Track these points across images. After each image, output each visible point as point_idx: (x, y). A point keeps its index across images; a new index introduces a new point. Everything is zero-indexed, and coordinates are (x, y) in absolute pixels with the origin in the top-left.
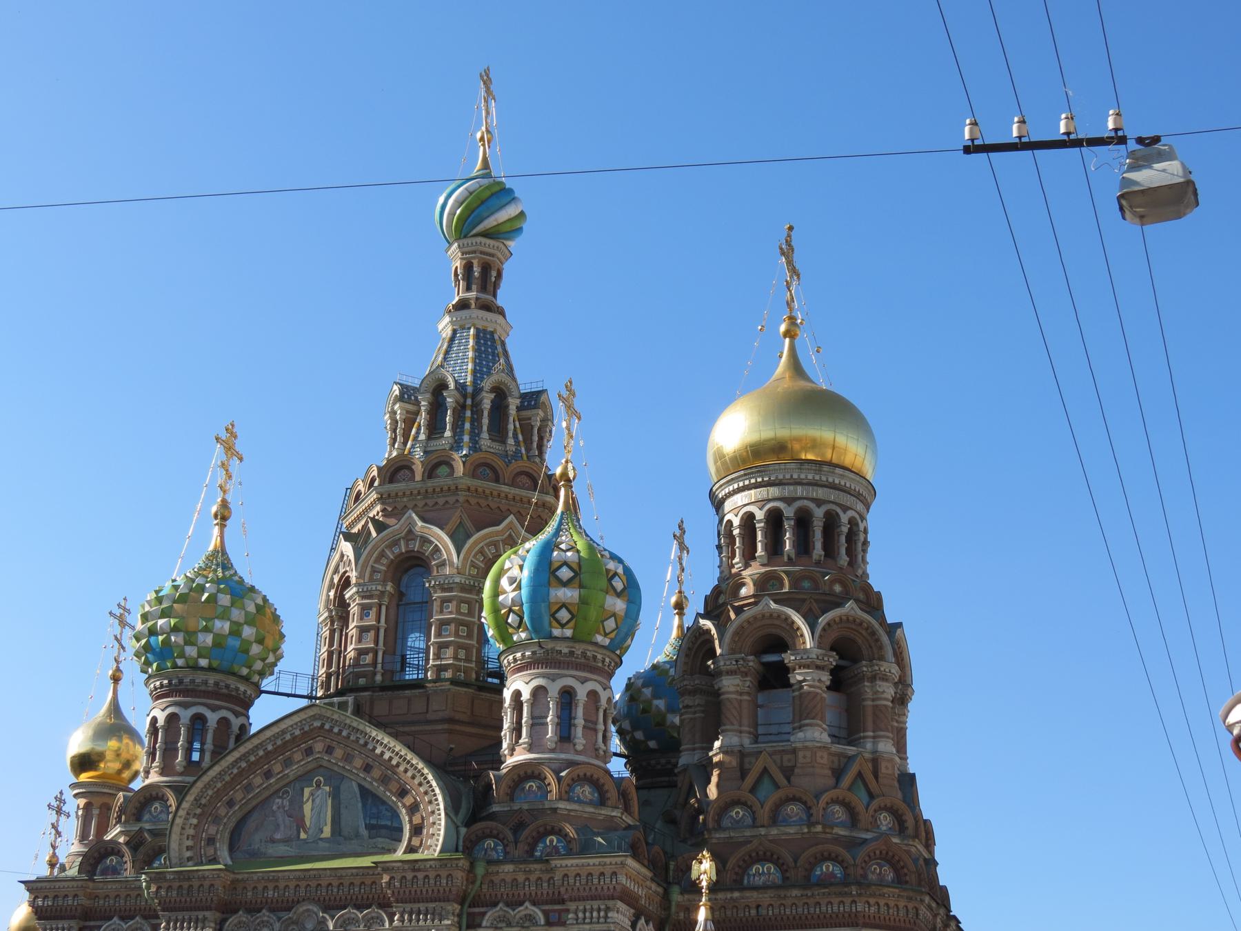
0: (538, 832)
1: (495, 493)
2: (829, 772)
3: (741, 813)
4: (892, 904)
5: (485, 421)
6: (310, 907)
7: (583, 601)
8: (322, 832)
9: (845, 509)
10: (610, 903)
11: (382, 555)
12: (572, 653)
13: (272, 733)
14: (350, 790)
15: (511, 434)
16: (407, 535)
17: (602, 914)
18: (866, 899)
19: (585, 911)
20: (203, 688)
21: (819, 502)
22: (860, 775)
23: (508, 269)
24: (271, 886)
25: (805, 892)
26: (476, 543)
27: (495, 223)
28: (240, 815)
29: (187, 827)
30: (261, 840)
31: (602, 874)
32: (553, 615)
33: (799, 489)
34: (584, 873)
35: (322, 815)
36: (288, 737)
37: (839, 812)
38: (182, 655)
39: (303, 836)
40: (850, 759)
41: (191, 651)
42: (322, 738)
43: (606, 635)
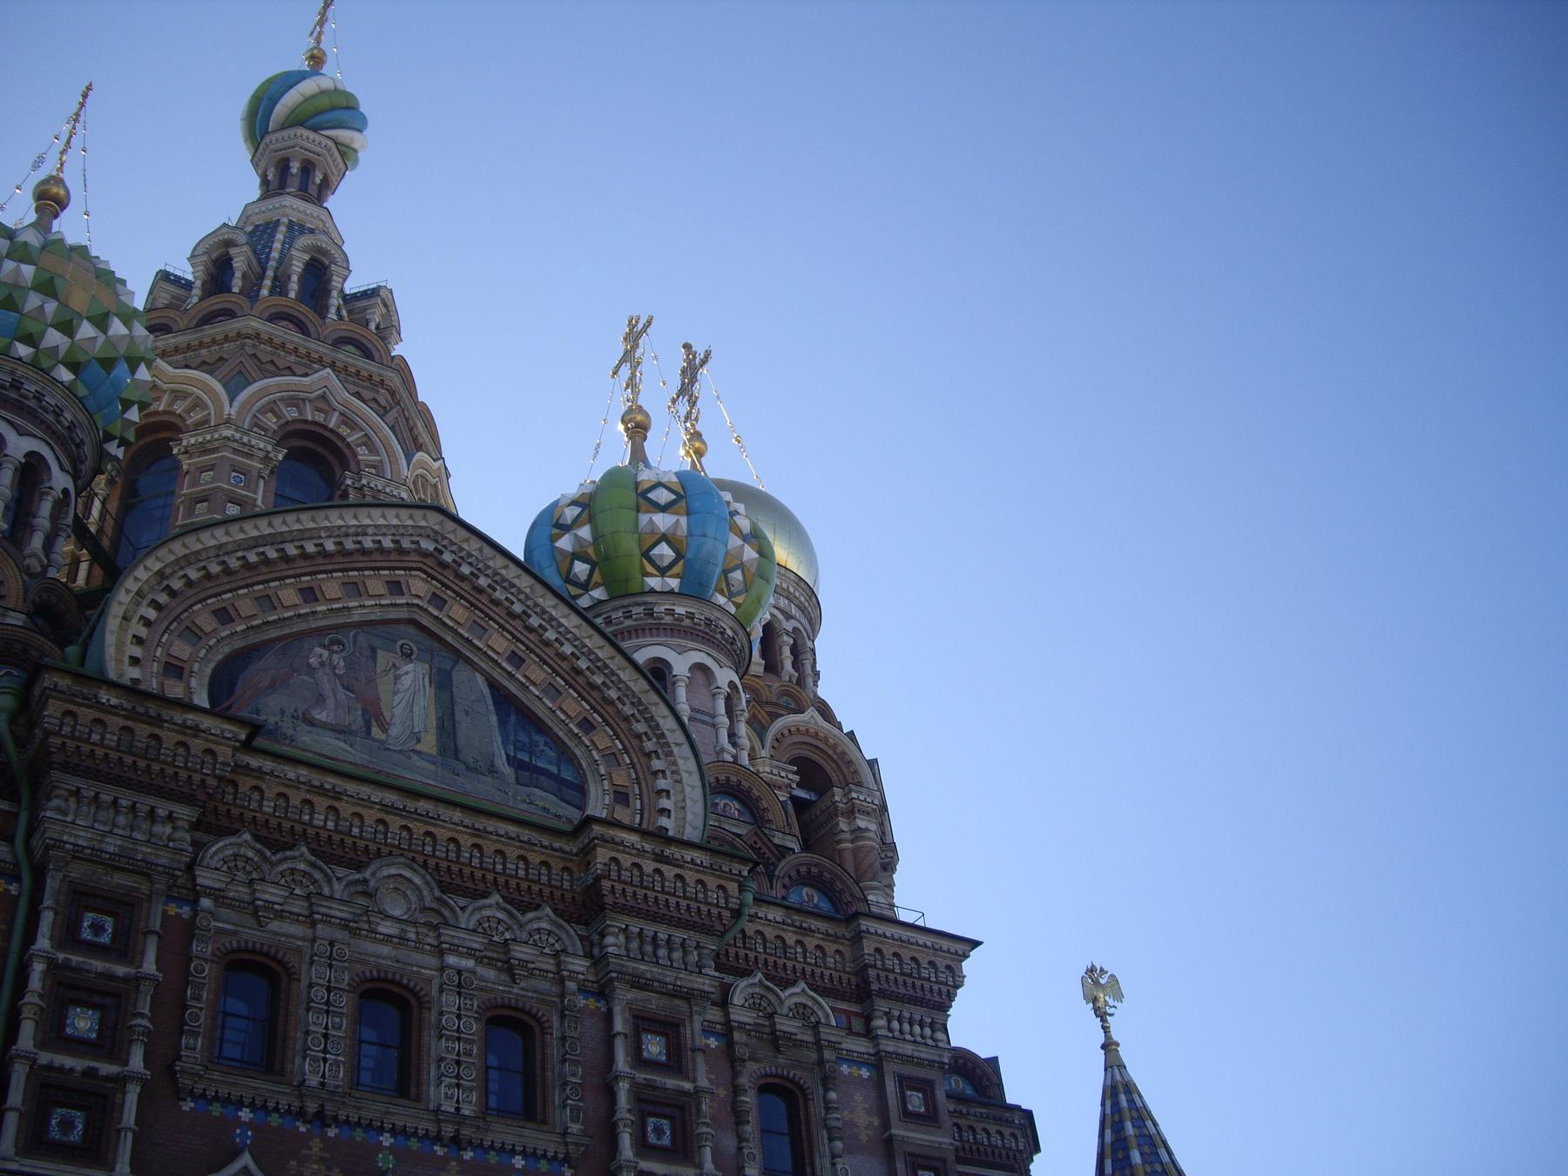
6: (407, 873)
8: (419, 741)
11: (271, 408)
13: (340, 523)
14: (471, 688)
20: (50, 418)
24: (321, 803)
27: (347, 142)
28: (238, 644)
29: (135, 620)
30: (283, 712)
31: (931, 963)
32: (725, 572)
33: (794, 610)
35: (416, 709)
36: (368, 543)
42: (424, 576)
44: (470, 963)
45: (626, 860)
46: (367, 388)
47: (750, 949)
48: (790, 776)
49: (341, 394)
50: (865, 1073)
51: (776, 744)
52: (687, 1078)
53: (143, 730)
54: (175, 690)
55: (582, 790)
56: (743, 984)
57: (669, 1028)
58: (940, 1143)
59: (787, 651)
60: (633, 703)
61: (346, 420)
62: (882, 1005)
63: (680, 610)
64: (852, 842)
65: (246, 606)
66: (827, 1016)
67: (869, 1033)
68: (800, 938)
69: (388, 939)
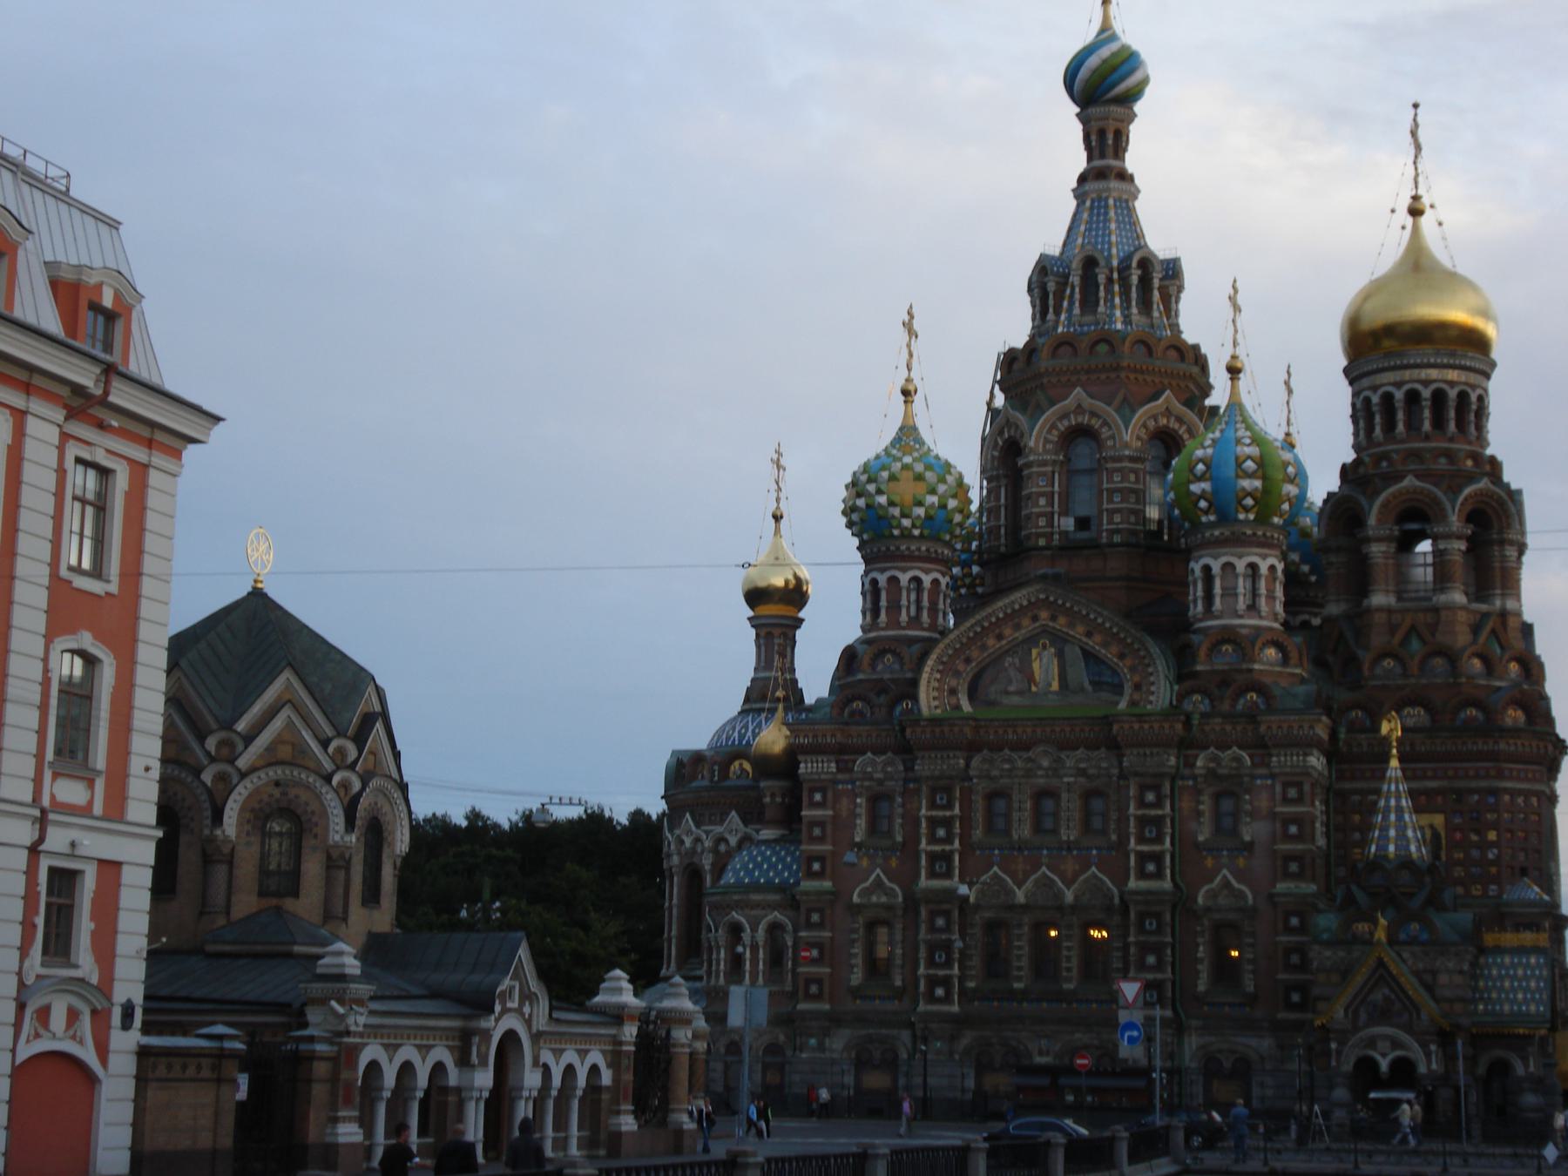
1: (1151, 368)
2: (1468, 629)
3: (1392, 664)
4: (1527, 743)
5: (1134, 295)
7: (1266, 490)
9: (1474, 387)
11: (1053, 426)
12: (1254, 534)
14: (1073, 653)
15: (1155, 306)
16: (1077, 408)
17: (1301, 758)
19: (1286, 755)
20: (917, 553)
21: (1452, 384)
22: (1493, 631)
23: (1135, 130)
26: (1140, 417)
29: (932, 681)
33: (1433, 373)
34: (1285, 726)
38: (899, 526)
39: (1034, 689)
40: (1485, 616)
41: (906, 522)
43: (1281, 516)
44: (1072, 779)
45: (1126, 726)
49: (1088, 402)
50: (1269, 782)
53: (937, 730)
54: (954, 701)
57: (1157, 788)
59: (1427, 413)
61: (1093, 414)
62: (1274, 751)
63: (1217, 533)
65: (975, 653)
67: (1268, 765)
69: (1042, 776)
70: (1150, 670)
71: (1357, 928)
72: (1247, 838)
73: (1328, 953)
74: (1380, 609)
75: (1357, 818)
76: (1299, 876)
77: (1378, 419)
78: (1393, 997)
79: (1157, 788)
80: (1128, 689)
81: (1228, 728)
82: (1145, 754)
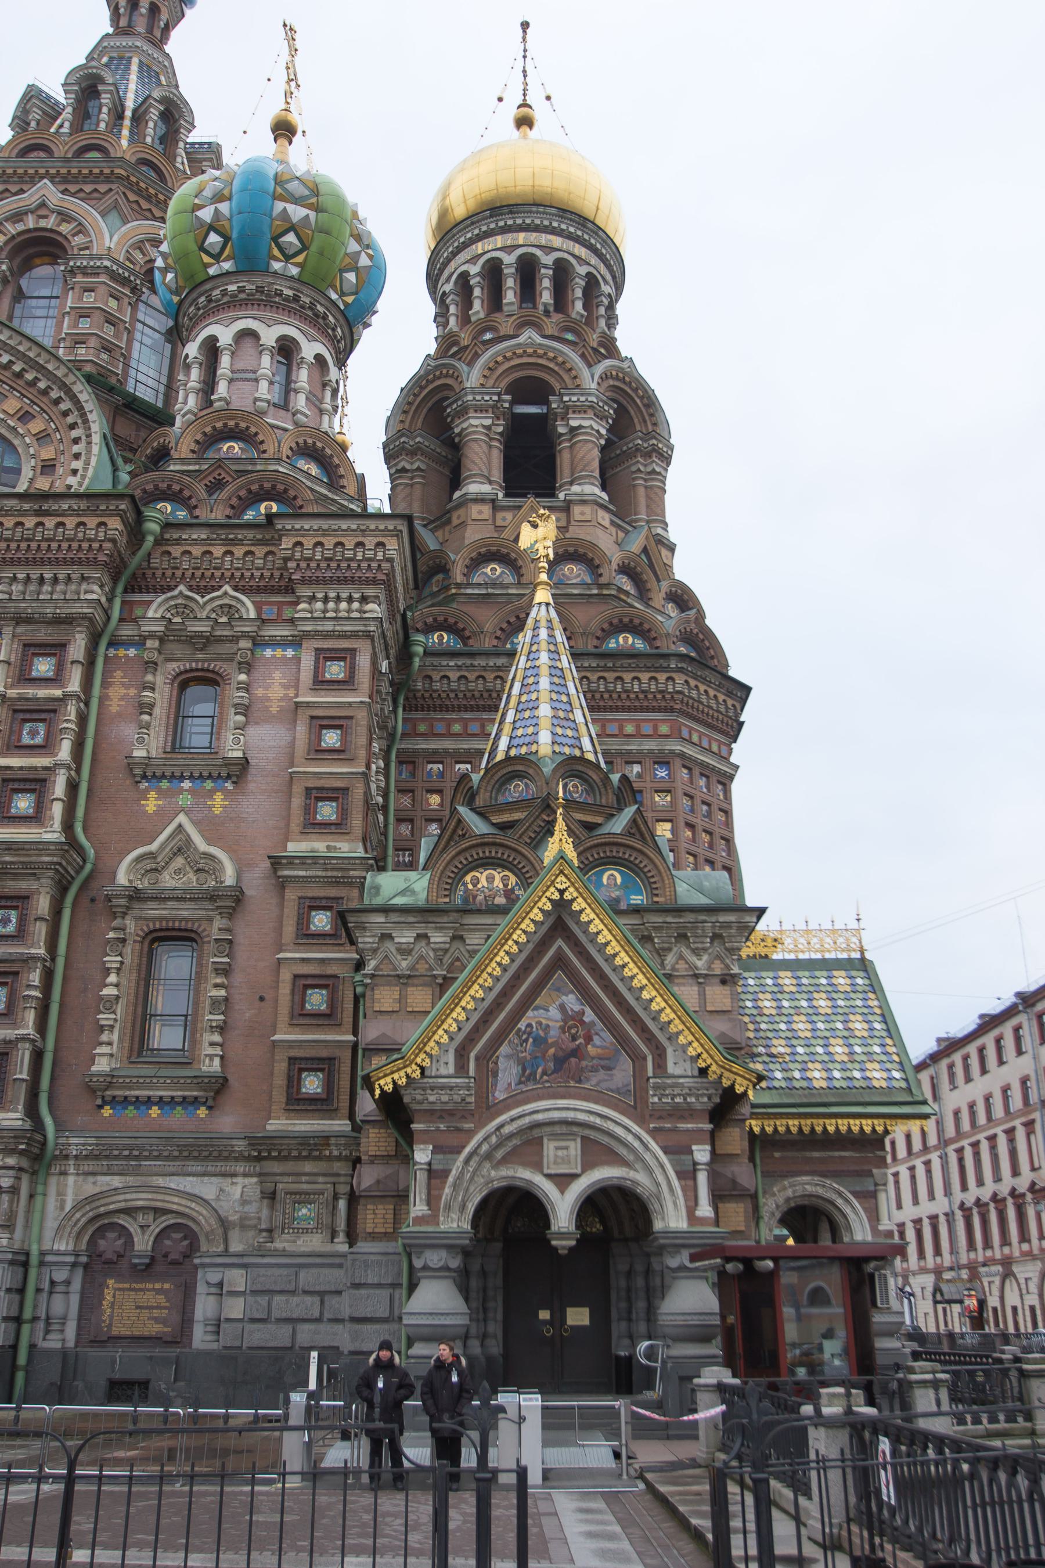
0: (250, 491)
3: (499, 571)
4: (712, 693)
9: (606, 282)
10: (370, 592)
12: (296, 299)
15: (179, 159)
17: (356, 605)
18: (685, 677)
19: (326, 600)
22: (645, 550)
25: (602, 664)
32: (275, 239)
33: (557, 241)
34: (329, 542)
37: (626, 584)
43: (342, 294)
46: (103, 182)
47: (177, 568)
48: (495, 398)
50: (290, 653)
51: (487, 373)
52: (63, 686)
55: (18, 471)
56: (164, 597)
57: (56, 649)
58: (350, 703)
59: (546, 283)
60: (60, 389)
61: (65, 216)
62: (305, 592)
63: (232, 288)
64: (570, 440)
66: (248, 610)
68: (229, 548)
70: (74, 434)
71: (476, 882)
72: (240, 754)
73: (405, 937)
74: (479, 500)
75: (435, 800)
76: (337, 828)
77: (477, 292)
78: (589, 1016)
79: (56, 649)
80: (27, 473)
81: (218, 551)
82: (42, 580)
